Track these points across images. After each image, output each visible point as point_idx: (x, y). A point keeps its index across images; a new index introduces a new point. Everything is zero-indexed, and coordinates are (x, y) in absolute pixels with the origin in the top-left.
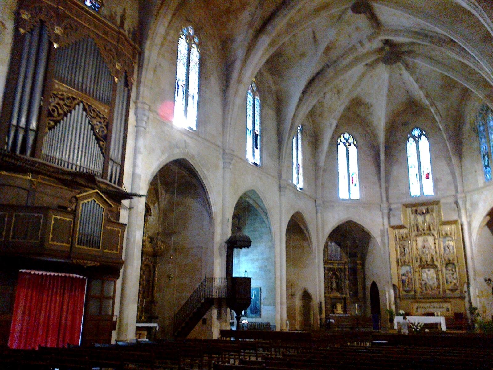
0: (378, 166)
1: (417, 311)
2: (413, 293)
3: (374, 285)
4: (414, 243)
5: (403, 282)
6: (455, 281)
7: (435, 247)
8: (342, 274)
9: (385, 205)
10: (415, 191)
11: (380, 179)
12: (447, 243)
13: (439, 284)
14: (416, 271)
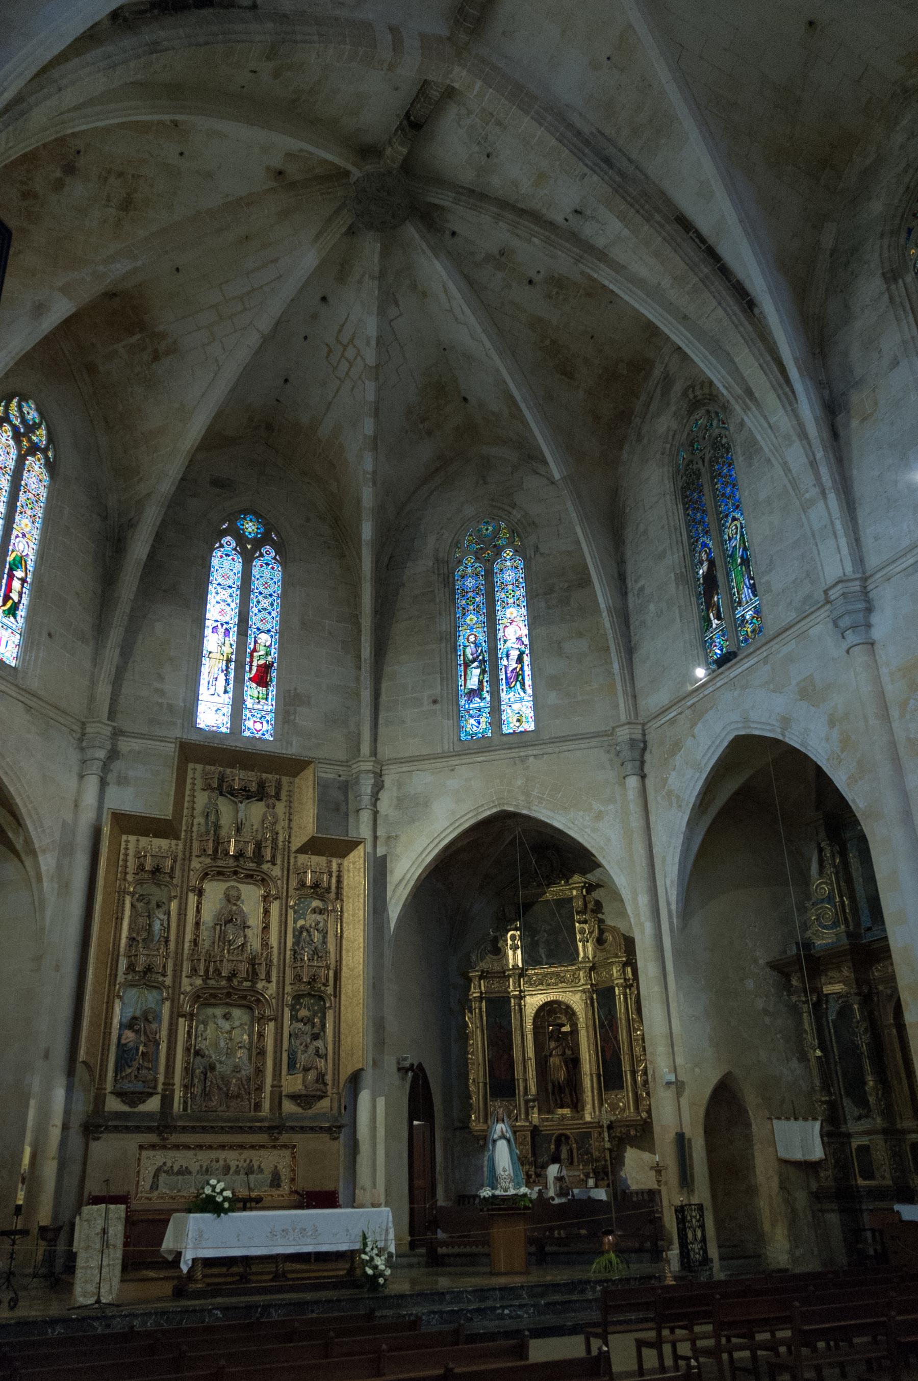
4: (192, 899)
5: (125, 1055)
13: (259, 1071)
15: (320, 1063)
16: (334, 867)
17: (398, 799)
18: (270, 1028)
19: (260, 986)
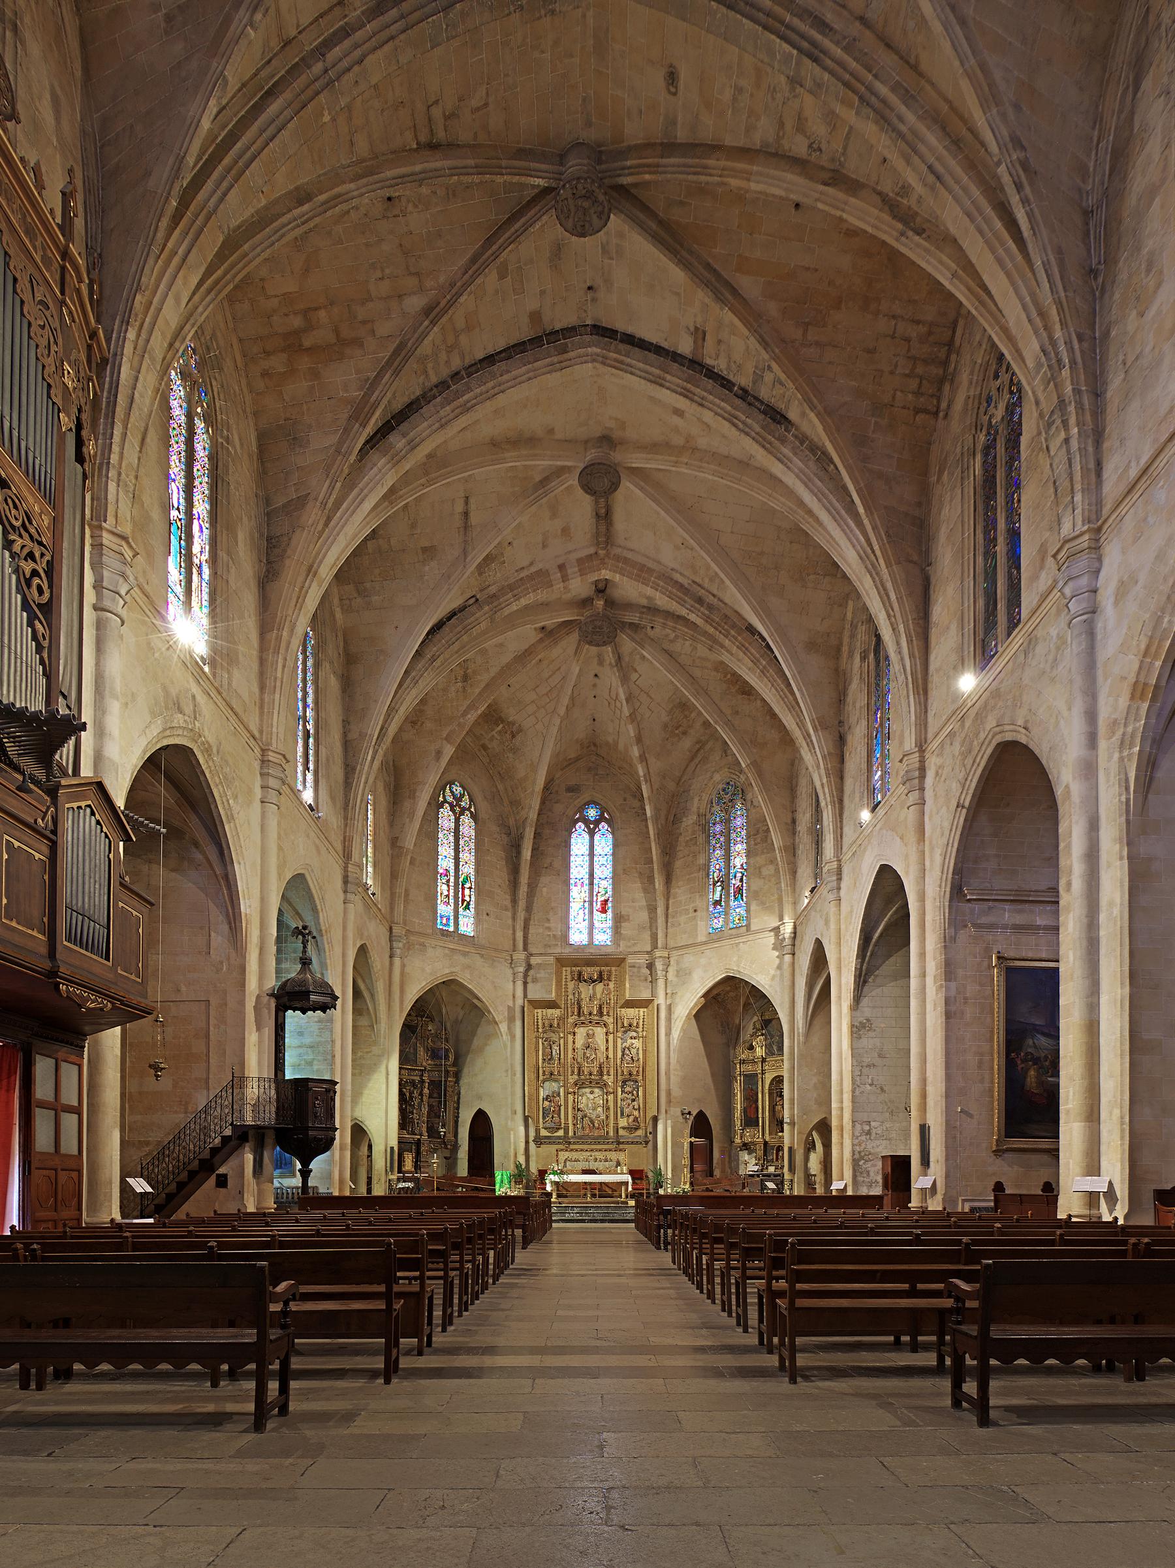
0: (515, 871)
1: (565, 1166)
2: (561, 1133)
3: (481, 1122)
4: (570, 1037)
6: (636, 1113)
7: (607, 1049)
8: (416, 1094)
9: (520, 956)
10: (578, 936)
11: (514, 901)
12: (629, 1041)
14: (568, 1093)
15: (636, 1113)
16: (642, 1014)
17: (678, 971)
18: (611, 1097)
19: (605, 1077)
